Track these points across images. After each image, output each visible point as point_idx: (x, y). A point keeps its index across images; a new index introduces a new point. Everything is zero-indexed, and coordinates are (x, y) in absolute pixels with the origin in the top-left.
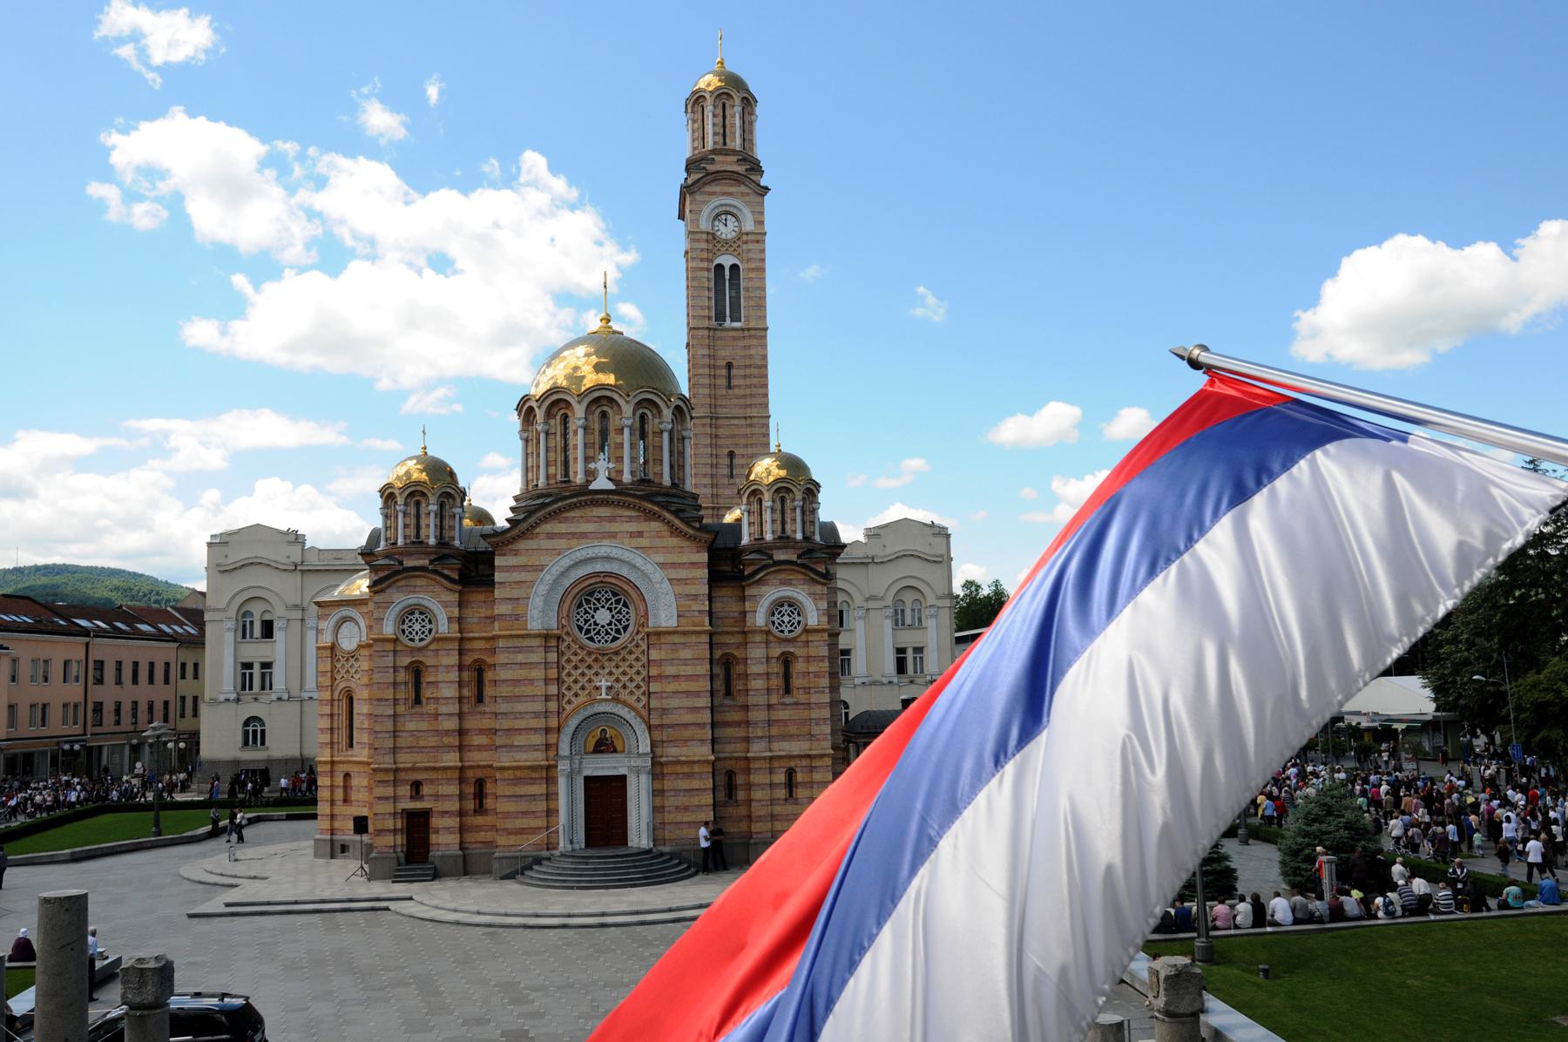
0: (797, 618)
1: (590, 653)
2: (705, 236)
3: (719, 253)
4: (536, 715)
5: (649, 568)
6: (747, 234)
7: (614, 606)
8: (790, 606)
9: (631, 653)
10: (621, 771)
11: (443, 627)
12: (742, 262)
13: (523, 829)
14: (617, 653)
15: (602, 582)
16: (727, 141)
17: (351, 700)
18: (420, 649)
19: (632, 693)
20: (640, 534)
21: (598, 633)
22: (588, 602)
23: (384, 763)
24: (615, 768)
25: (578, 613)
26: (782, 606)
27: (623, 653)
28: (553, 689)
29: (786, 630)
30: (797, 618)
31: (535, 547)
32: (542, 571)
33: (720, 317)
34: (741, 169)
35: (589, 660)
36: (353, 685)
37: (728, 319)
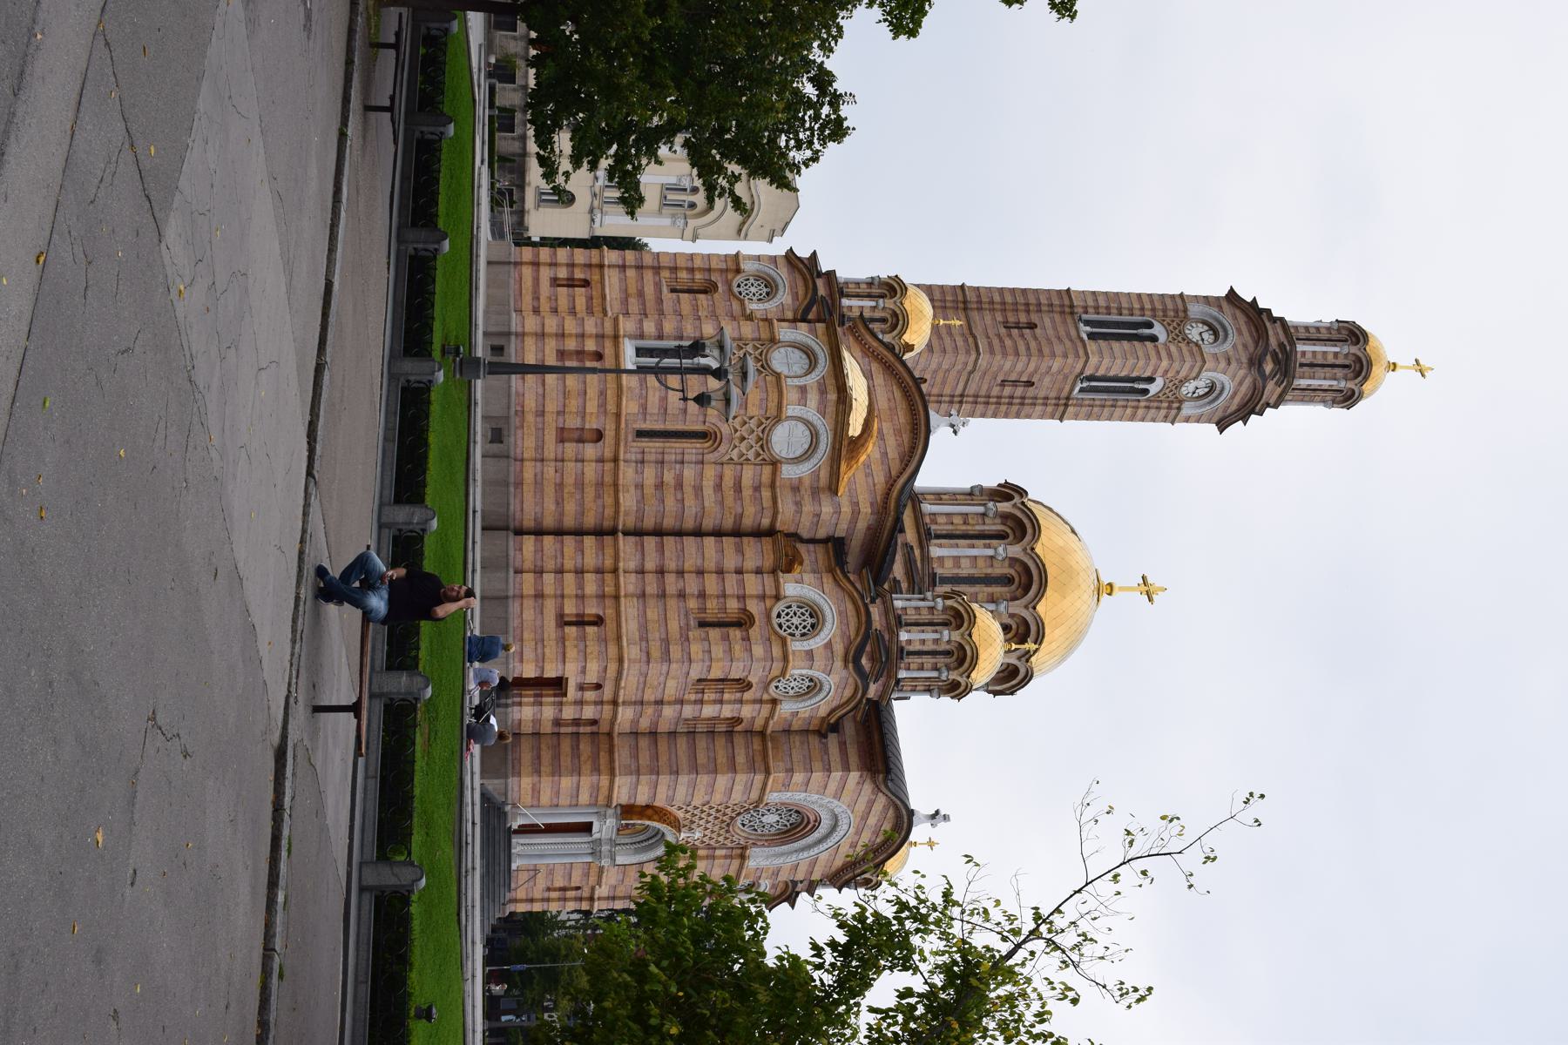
2: (1194, 374)
3: (1167, 381)
4: (671, 799)
5: (816, 850)
6: (1179, 409)
9: (726, 838)
10: (596, 836)
12: (1147, 400)
13: (539, 792)
16: (1296, 393)
17: (703, 435)
18: (766, 688)
20: (853, 845)
23: (627, 675)
24: (600, 831)
28: (697, 802)
31: (862, 793)
33: (1091, 378)
34: (1258, 408)
36: (722, 449)
37: (1085, 385)
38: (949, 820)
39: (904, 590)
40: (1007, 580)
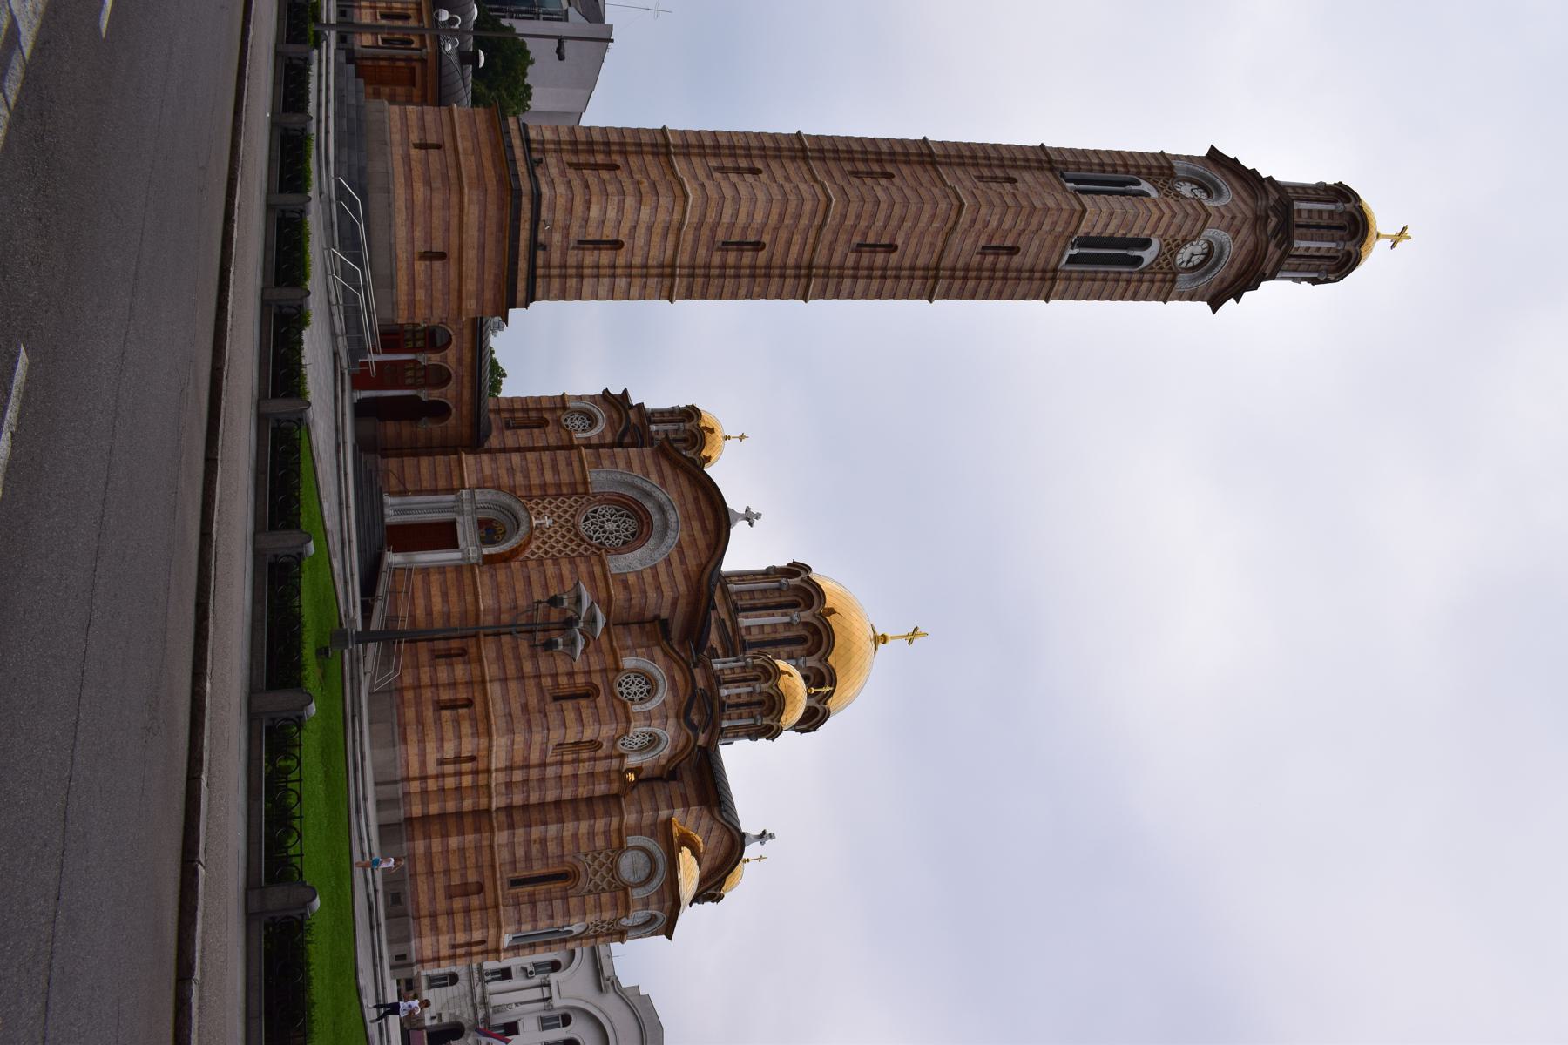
0: (636, 698)
1: (573, 516)
7: (623, 534)
8: (648, 691)
11: (579, 436)
14: (577, 535)
15: (642, 521)
19: (539, 548)
21: (593, 524)
22: (622, 516)
25: (609, 509)
26: (647, 683)
27: (578, 540)
29: (623, 689)
30: (636, 698)
32: (644, 476)
35: (567, 516)
38: (760, 514)
39: (720, 656)
40: (800, 640)
